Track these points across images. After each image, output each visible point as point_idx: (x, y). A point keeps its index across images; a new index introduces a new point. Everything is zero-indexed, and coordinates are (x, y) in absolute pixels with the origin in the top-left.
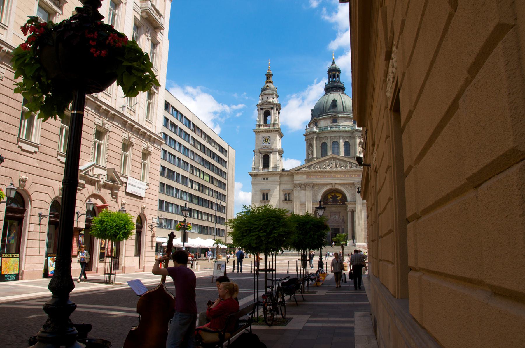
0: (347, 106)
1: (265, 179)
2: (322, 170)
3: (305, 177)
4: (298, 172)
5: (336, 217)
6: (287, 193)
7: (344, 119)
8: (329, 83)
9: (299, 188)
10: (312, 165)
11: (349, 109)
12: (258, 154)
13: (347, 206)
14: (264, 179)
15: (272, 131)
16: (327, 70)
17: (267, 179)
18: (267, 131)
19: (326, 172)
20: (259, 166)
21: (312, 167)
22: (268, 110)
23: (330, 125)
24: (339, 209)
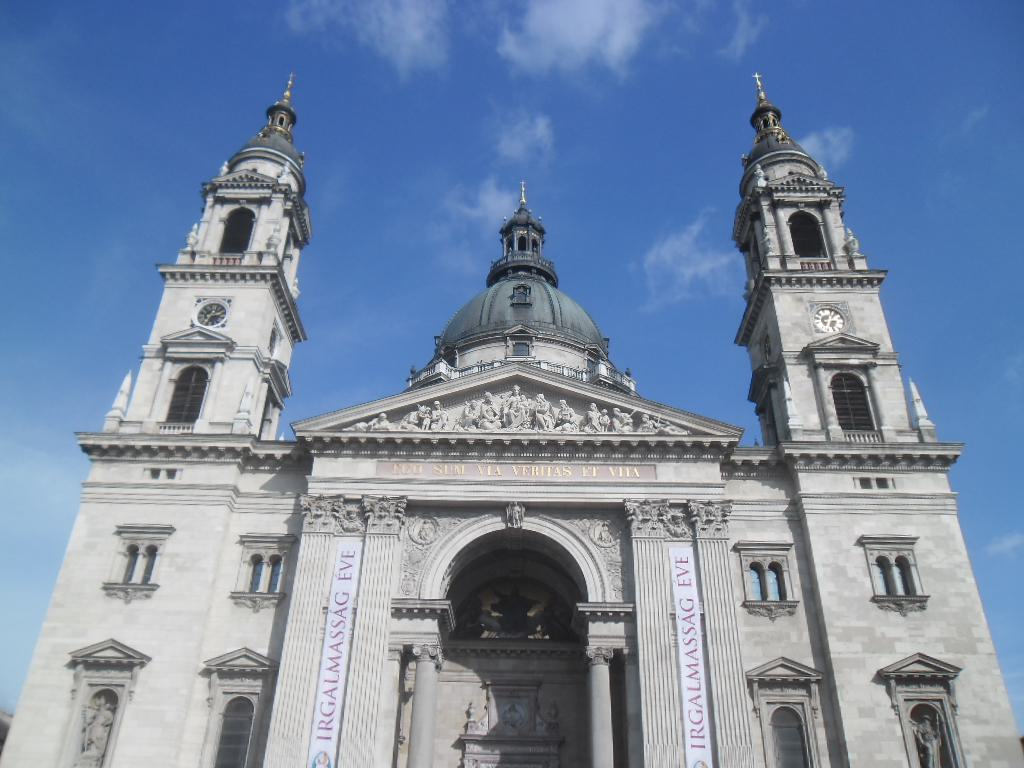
1: (163, 474)
2: (461, 430)
3: (366, 467)
5: (517, 707)
6: (262, 552)
7: (558, 347)
9: (333, 520)
10: (414, 407)
12: (158, 363)
14: (155, 473)
15: (243, 276)
17: (171, 474)
18: (223, 276)
19: (481, 445)
20: (150, 415)
22: (248, 207)
24: (534, 665)
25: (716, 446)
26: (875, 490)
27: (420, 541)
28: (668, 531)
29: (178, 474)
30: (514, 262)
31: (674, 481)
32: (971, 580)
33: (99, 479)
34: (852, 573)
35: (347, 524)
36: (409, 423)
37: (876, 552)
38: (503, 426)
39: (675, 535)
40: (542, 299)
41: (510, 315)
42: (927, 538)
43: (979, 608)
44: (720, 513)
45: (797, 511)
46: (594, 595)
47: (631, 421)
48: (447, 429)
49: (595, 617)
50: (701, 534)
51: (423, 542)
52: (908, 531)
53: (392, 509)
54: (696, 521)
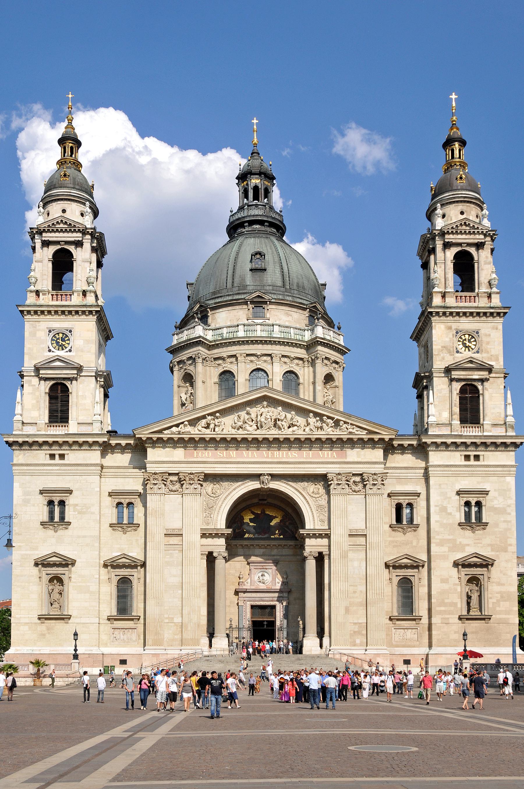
0: (293, 275)
1: (57, 457)
2: (234, 431)
3: (179, 454)
4: (158, 439)
8: (241, 208)
9: (163, 486)
10: (204, 417)
11: (298, 284)
13: (302, 547)
14: (52, 456)
16: (237, 173)
17: (62, 456)
19: (244, 440)
21: (203, 422)
23: (246, 322)
25: (382, 440)
26: (472, 462)
27: (212, 495)
28: (351, 489)
29: (66, 456)
30: (250, 216)
31: (356, 460)
32: (514, 514)
33: (20, 462)
34: (449, 511)
35: (171, 487)
36: (202, 427)
37: (466, 498)
38: (258, 428)
39: (355, 491)
40: (274, 263)
41: (249, 279)
42: (495, 490)
43: (514, 529)
44: (380, 479)
45: (427, 473)
46: (309, 525)
47: (333, 424)
48: (225, 432)
49: (309, 536)
50: (369, 491)
51: (214, 496)
52: (487, 487)
53: (196, 479)
54: (367, 484)
